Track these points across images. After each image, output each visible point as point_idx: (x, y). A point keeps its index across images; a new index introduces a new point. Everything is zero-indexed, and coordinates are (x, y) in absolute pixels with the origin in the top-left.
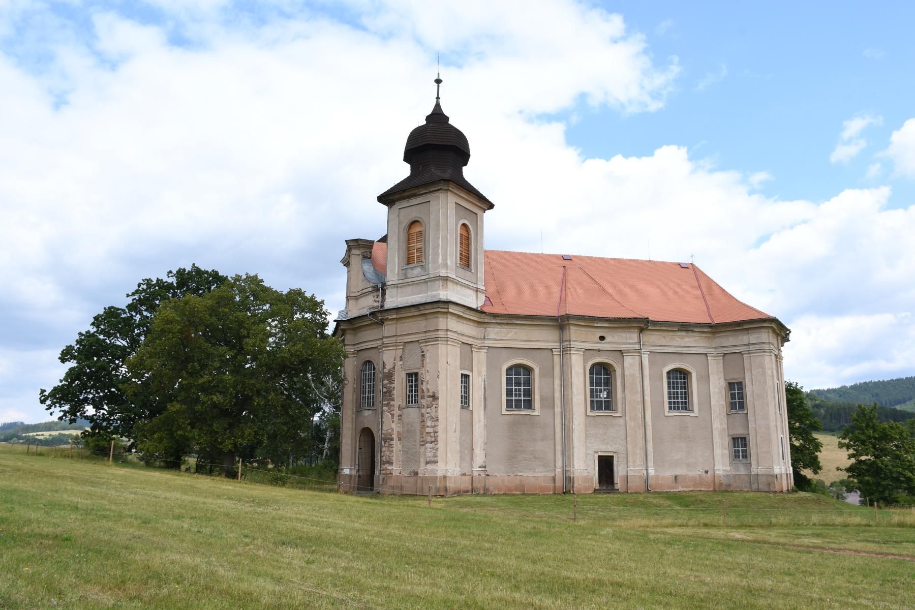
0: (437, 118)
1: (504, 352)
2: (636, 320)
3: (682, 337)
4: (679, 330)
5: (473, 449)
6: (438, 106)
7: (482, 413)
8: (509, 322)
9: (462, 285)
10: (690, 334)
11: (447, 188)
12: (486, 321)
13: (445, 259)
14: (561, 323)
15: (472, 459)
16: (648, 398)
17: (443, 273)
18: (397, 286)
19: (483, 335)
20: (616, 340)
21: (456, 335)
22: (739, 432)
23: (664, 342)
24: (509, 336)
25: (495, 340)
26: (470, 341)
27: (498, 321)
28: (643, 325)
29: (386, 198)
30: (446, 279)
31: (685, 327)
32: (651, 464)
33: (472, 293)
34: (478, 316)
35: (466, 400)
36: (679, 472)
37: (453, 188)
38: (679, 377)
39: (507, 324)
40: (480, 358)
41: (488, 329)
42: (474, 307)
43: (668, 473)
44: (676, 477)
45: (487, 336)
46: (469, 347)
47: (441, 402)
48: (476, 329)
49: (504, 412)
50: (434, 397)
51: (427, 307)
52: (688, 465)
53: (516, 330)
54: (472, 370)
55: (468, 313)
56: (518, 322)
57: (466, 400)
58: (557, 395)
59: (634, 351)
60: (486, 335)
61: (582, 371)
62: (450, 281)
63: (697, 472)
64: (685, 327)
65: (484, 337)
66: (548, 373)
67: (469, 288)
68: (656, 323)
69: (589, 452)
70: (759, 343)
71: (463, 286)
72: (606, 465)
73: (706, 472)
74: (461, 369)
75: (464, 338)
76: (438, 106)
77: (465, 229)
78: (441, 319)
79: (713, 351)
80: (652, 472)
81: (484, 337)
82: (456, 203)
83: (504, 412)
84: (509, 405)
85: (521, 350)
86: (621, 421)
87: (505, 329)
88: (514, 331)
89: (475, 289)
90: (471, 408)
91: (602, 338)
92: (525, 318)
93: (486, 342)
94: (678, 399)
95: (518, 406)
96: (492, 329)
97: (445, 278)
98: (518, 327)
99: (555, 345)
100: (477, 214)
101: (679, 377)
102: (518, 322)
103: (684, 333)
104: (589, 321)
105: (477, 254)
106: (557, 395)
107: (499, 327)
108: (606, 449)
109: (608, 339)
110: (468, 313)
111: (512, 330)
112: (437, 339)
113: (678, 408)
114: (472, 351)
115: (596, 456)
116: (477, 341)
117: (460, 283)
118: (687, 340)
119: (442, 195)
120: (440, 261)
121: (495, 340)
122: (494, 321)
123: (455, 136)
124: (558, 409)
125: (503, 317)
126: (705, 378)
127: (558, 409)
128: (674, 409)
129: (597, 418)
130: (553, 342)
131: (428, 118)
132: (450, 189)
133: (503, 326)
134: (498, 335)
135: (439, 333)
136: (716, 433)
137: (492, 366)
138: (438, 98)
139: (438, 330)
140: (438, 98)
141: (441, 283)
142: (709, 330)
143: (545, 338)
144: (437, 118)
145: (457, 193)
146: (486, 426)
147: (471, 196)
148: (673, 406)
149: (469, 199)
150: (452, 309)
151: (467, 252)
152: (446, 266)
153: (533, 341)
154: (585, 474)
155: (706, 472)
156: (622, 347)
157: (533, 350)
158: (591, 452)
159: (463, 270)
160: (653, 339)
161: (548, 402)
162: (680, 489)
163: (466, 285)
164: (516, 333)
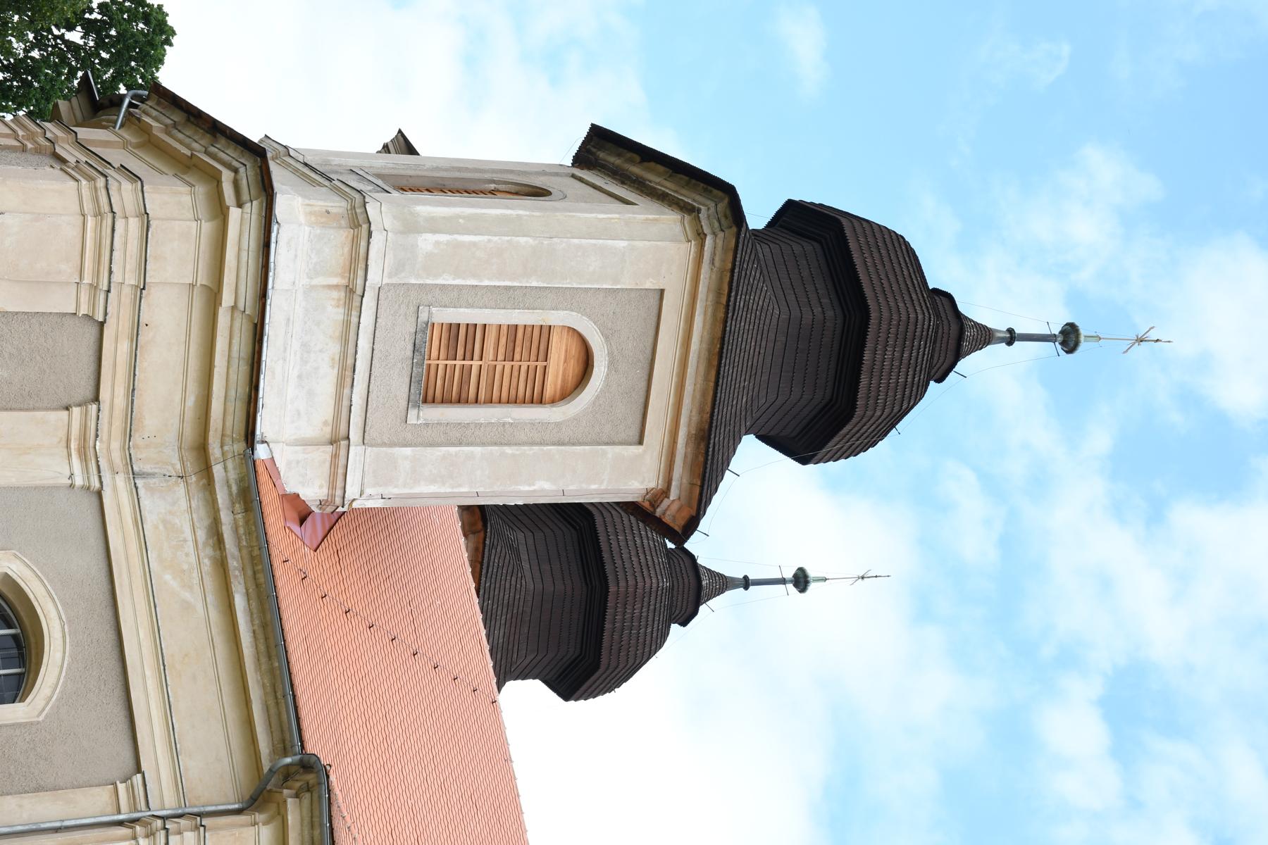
1: (91, 562)
8: (233, 564)
9: (349, 334)
11: (706, 230)
12: (217, 470)
13: (434, 226)
19: (147, 468)
21: (132, 279)
24: (168, 577)
25: (139, 521)
27: (225, 517)
30: (359, 223)
33: (318, 419)
34: (229, 424)
37: (712, 262)
39: (221, 565)
41: (181, 490)
45: (146, 487)
46: (86, 391)
48: (171, 436)
53: (199, 606)
55: (235, 348)
56: (240, 602)
60: (152, 481)
62: (355, 241)
65: (144, 475)
67: (340, 384)
71: (345, 342)
75: (124, 347)
77: (571, 380)
78: (187, 199)
81: (144, 475)
82: (662, 291)
85: (109, 636)
87: (193, 559)
88: (194, 598)
89: (343, 432)
92: (264, 626)
93: (121, 481)
96: (183, 504)
97: (361, 218)
98: (215, 615)
99: (164, 798)
100: (640, 442)
102: (240, 602)
105: (483, 444)
107: (201, 535)
110: (235, 348)
111: (197, 589)
114: (67, 409)
116: (116, 445)
117: (354, 320)
121: (139, 521)
122: (222, 497)
123: (904, 317)
125: (249, 533)
132: (709, 241)
133: (209, 551)
135: (127, 186)
145: (702, 289)
147: (706, 379)
149: (691, 370)
150: (242, 222)
151: (482, 396)
152: (411, 227)
153: (164, 684)
157: (118, 692)
159: (409, 353)
163: (350, 361)
164: (187, 607)
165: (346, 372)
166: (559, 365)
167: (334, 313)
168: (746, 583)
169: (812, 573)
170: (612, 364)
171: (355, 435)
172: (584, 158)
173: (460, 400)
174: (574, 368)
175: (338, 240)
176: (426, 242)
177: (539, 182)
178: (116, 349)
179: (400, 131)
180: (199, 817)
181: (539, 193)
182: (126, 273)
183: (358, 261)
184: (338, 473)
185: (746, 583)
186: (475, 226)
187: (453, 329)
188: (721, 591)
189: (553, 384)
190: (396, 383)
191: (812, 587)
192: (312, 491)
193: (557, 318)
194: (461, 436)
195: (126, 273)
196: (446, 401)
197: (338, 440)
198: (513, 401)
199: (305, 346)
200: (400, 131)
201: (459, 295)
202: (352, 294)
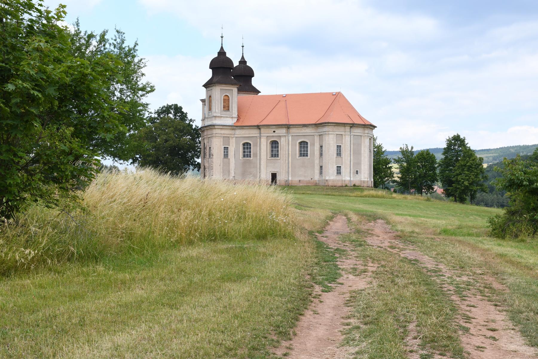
0: (222, 53)
3: (305, 130)
4: (303, 127)
5: (229, 171)
6: (222, 48)
7: (234, 159)
9: (224, 117)
10: (308, 128)
13: (215, 110)
14: (258, 127)
15: (229, 174)
16: (290, 153)
17: (215, 115)
20: (279, 132)
22: (321, 164)
26: (228, 136)
28: (288, 127)
29: (206, 86)
30: (215, 117)
31: (305, 126)
32: (290, 176)
33: (230, 119)
35: (226, 155)
36: (301, 179)
38: (303, 145)
39: (242, 129)
40: (233, 142)
43: (297, 179)
44: (300, 180)
47: (214, 157)
49: (241, 159)
50: (213, 155)
51: (210, 126)
52: (305, 176)
54: (229, 145)
57: (226, 155)
58: (258, 152)
61: (265, 144)
63: (308, 179)
64: (305, 126)
66: (256, 145)
69: (268, 171)
70: (325, 131)
72: (274, 176)
73: (312, 179)
74: (223, 145)
76: (222, 48)
79: (317, 134)
80: (290, 179)
83: (241, 159)
84: (244, 156)
86: (279, 161)
90: (229, 158)
91: (274, 132)
94: (302, 152)
95: (247, 157)
99: (258, 135)
101: (303, 145)
103: (306, 128)
106: (258, 152)
108: (274, 171)
112: (212, 137)
113: (302, 156)
115: (271, 173)
118: (307, 130)
120: (214, 111)
124: (258, 157)
126: (313, 144)
127: (258, 157)
128: (303, 156)
129: (271, 160)
130: (257, 134)
131: (219, 53)
134: (240, 133)
136: (316, 165)
137: (237, 143)
138: (222, 44)
139: (213, 134)
140: (222, 44)
141: (214, 118)
142: (315, 126)
143: (254, 133)
144: (222, 53)
146: (235, 164)
148: (301, 155)
152: (215, 112)
154: (266, 179)
155: (312, 179)
158: (269, 172)
160: (293, 130)
161: (255, 155)
162: (301, 185)
166: (226, 98)
167: (222, 118)
168: (243, 54)
169: (242, 45)
170: (226, 93)
171: (232, 116)
173: (229, 106)
174: (226, 96)
175: (217, 118)
176: (217, 111)
177: (209, 97)
178: (225, 135)
179: (201, 100)
180: (260, 133)
181: (210, 96)
182: (220, 135)
183: (219, 117)
184: (235, 117)
185: (243, 54)
186: (215, 106)
187: (223, 108)
189: (228, 98)
190: (228, 113)
191: (244, 45)
192: (236, 120)
193: (222, 99)
195: (220, 135)
196: (229, 108)
197: (232, 117)
198: (229, 102)
199: (225, 121)
200: (201, 100)
201: (221, 108)
202: (221, 117)
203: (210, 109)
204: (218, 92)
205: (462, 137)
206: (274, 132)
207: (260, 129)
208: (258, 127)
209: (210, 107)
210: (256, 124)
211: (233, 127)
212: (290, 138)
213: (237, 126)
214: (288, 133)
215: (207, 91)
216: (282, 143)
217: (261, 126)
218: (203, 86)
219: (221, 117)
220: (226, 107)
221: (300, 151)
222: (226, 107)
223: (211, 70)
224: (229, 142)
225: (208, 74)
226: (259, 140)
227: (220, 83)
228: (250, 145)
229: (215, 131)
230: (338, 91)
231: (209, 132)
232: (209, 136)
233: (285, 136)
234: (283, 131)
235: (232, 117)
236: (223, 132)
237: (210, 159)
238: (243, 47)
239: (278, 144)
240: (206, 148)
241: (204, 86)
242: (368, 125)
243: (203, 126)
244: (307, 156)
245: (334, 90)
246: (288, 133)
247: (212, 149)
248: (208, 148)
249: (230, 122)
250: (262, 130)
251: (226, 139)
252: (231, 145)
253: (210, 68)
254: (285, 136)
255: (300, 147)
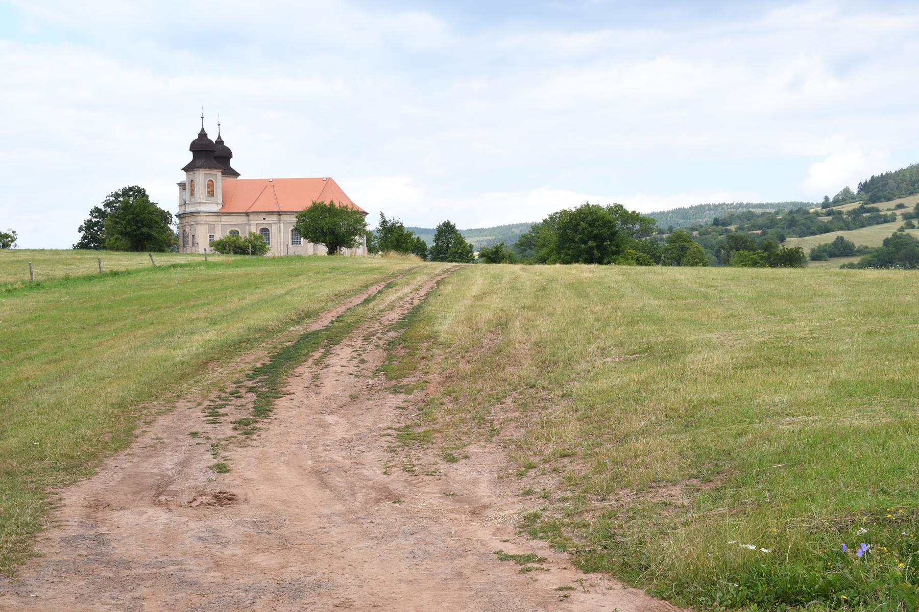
0: (203, 135)
2: (277, 212)
6: (203, 129)
9: (209, 203)
13: (200, 196)
14: (247, 214)
16: (282, 240)
17: (199, 201)
18: (188, 204)
23: (289, 219)
26: (214, 223)
28: (279, 214)
29: (187, 169)
30: (200, 203)
33: (215, 205)
42: (216, 211)
47: (199, 245)
54: (215, 233)
59: (276, 223)
68: (285, 212)
76: (203, 129)
91: (264, 219)
99: (247, 222)
104: (257, 213)
109: (266, 219)
112: (197, 224)
119: (198, 172)
131: (200, 135)
134: (225, 220)
144: (203, 135)
150: (201, 214)
152: (200, 198)
156: (272, 222)
165: (212, 203)
166: (211, 183)
167: (207, 204)
172: (186, 172)
175: (202, 205)
178: (210, 223)
184: (220, 204)
186: (199, 192)
188: (221, 139)
194: (217, 192)
197: (217, 203)
202: (206, 203)
203: (192, 194)
204: (201, 177)
205: (452, 223)
206: (264, 219)
207: (248, 216)
208: (247, 214)
209: (191, 190)
210: (244, 211)
211: (219, 214)
212: (282, 226)
213: (223, 213)
214: (279, 220)
215: (187, 176)
216: (274, 230)
217: (250, 212)
218: (183, 169)
219: (206, 203)
220: (211, 193)
221: (293, 239)
222: (211, 193)
223: (192, 153)
224: (214, 229)
225: (189, 157)
226: (247, 228)
227: (204, 167)
228: (238, 232)
229: (199, 218)
230: (328, 176)
231: (192, 219)
232: (192, 223)
233: (277, 223)
234: (275, 218)
235: (217, 203)
236: (208, 219)
237: (193, 248)
238: (219, 125)
239: (269, 231)
240: (188, 236)
241: (183, 169)
242: (361, 212)
243: (182, 212)
244: (300, 244)
245: (325, 176)
246: (279, 220)
247: (196, 237)
248: (190, 236)
249: (215, 208)
250: (251, 217)
251: (212, 226)
252: (216, 233)
253: (190, 150)
254: (277, 223)
255: (293, 235)
